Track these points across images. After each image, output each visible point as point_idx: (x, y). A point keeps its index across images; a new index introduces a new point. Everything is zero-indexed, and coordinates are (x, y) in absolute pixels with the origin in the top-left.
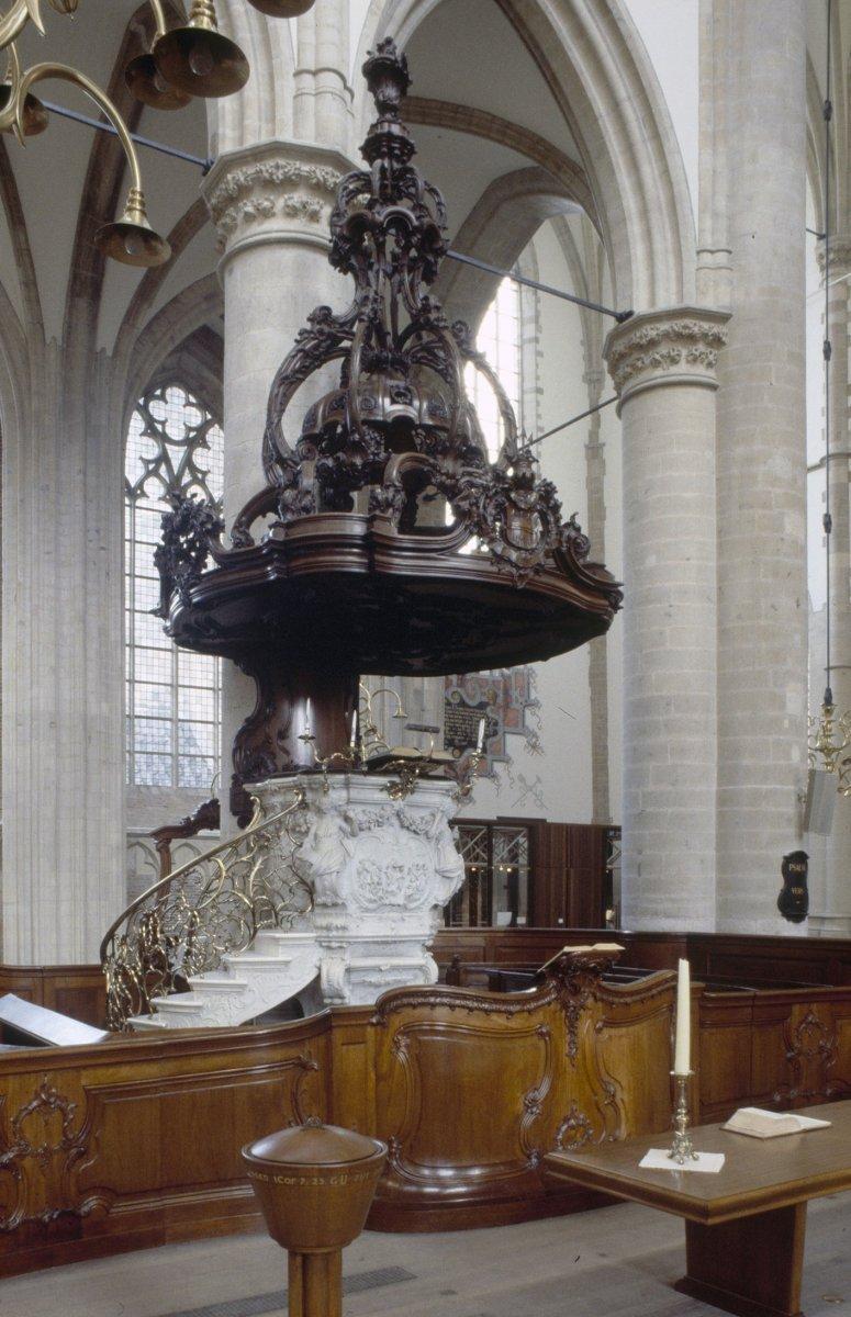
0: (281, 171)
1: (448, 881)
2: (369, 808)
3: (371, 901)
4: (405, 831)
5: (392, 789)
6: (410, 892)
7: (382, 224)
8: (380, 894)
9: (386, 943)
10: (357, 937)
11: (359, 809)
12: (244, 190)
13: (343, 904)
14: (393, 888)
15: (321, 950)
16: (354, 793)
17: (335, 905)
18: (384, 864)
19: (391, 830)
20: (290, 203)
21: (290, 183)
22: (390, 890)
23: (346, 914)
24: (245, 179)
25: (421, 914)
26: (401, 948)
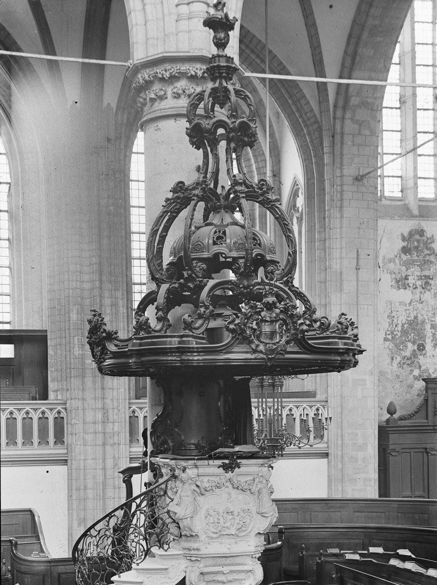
0: (168, 72)
1: (265, 518)
2: (211, 478)
3: (216, 533)
4: (236, 490)
5: (227, 468)
7: (211, 129)
8: (220, 528)
10: (206, 554)
11: (205, 479)
12: (148, 84)
14: (228, 525)
15: (187, 561)
17: (192, 536)
19: (227, 490)
20: (175, 90)
21: (173, 78)
22: (226, 526)
24: (149, 77)
26: (237, 560)
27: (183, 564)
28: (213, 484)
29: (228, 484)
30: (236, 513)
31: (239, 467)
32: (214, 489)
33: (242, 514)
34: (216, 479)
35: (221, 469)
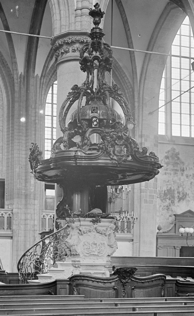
2: (86, 227)
3: (88, 254)
4: (98, 234)
5: (94, 222)
6: (99, 251)
8: (90, 251)
9: (92, 266)
13: (78, 254)
15: (74, 267)
16: (82, 223)
17: (76, 255)
18: (91, 243)
22: (93, 250)
23: (80, 257)
25: (104, 258)
26: (98, 268)
27: (72, 268)
28: (88, 230)
29: (95, 230)
30: (98, 244)
31: (100, 222)
32: (88, 232)
33: (101, 245)
34: (88, 227)
35: (92, 222)
